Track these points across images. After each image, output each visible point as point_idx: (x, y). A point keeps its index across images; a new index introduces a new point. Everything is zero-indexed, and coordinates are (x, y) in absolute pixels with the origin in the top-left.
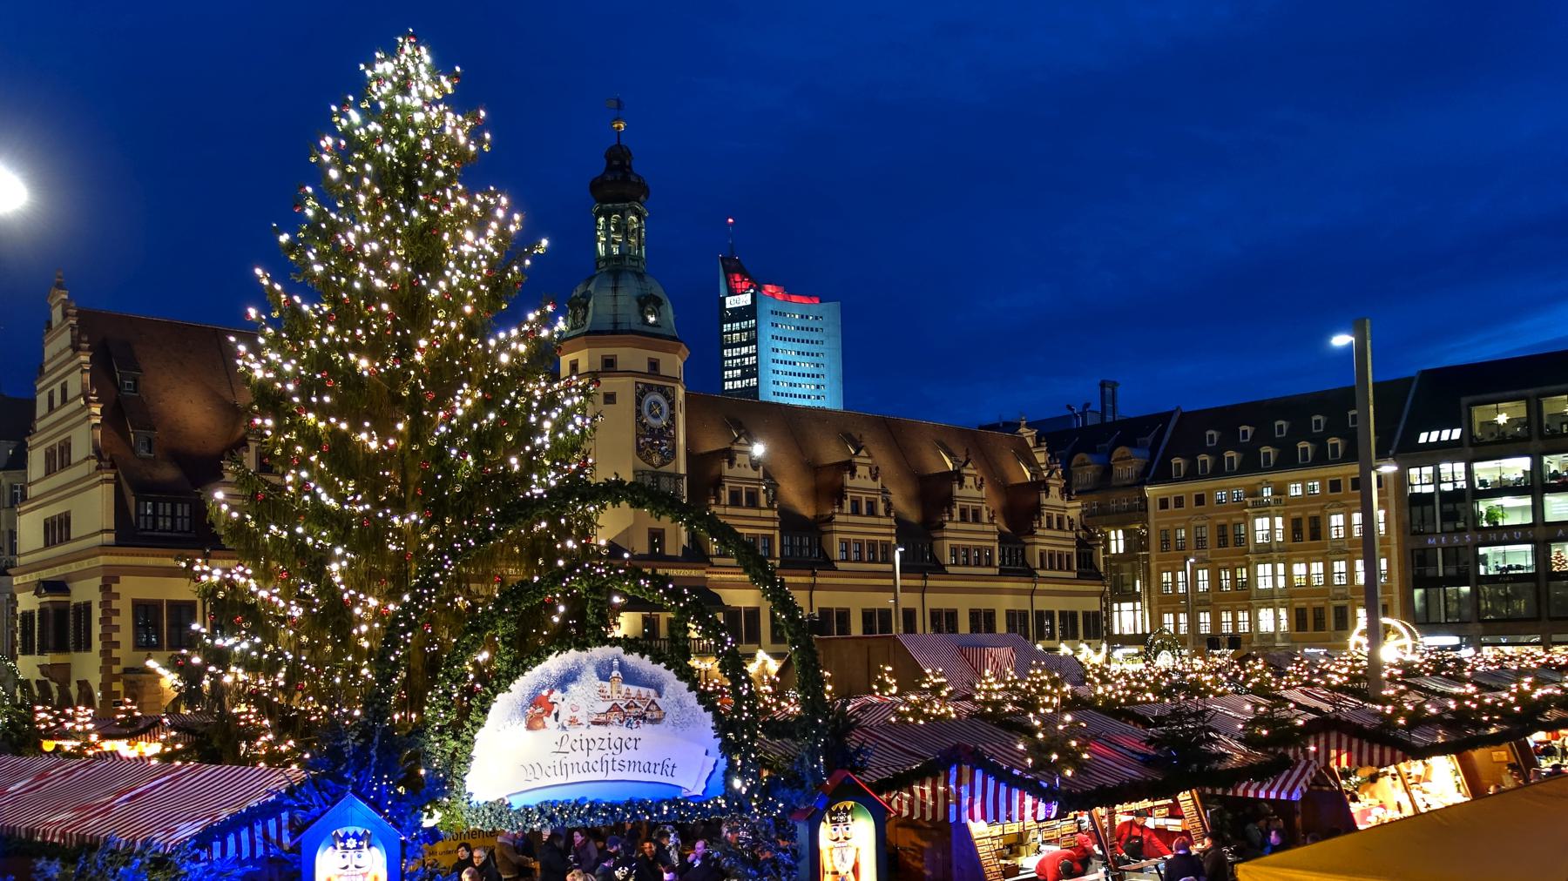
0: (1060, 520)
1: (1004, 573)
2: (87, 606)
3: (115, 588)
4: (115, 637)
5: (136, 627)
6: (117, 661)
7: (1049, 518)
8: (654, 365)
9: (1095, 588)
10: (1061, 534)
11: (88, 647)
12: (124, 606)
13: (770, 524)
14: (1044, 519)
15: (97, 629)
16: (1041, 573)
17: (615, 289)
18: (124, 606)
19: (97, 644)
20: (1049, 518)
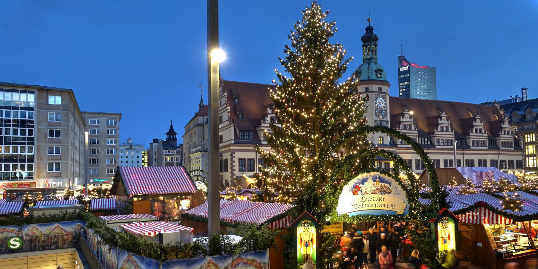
0: (508, 132)
1: (489, 149)
2: (227, 160)
3: (234, 155)
4: (234, 168)
5: (239, 165)
6: (235, 175)
7: (505, 131)
8: (380, 89)
9: (520, 153)
10: (508, 136)
11: (228, 171)
12: (236, 160)
13: (415, 135)
14: (503, 132)
15: (229, 166)
16: (502, 148)
17: (369, 68)
18: (236, 160)
19: (230, 170)
20: (505, 131)
